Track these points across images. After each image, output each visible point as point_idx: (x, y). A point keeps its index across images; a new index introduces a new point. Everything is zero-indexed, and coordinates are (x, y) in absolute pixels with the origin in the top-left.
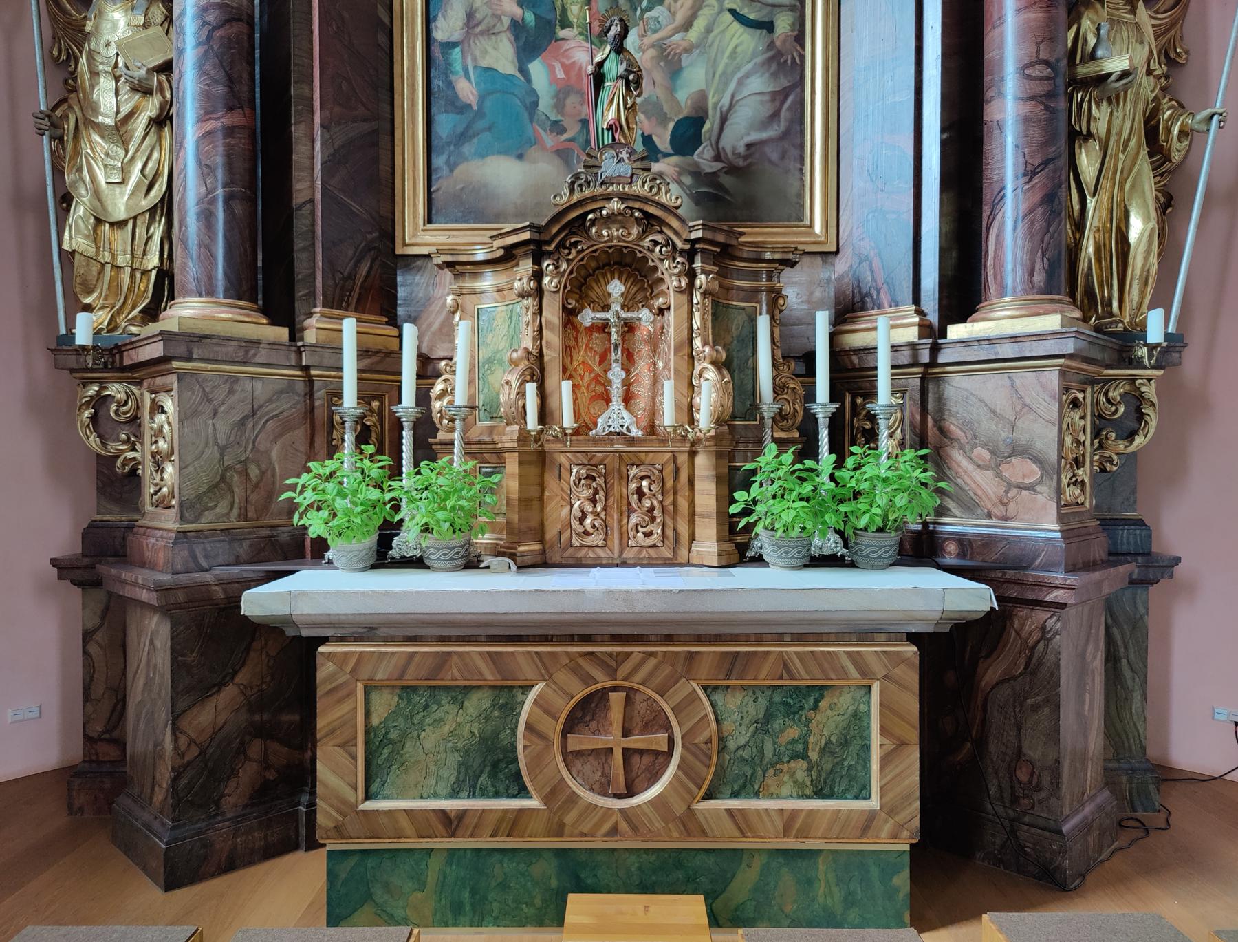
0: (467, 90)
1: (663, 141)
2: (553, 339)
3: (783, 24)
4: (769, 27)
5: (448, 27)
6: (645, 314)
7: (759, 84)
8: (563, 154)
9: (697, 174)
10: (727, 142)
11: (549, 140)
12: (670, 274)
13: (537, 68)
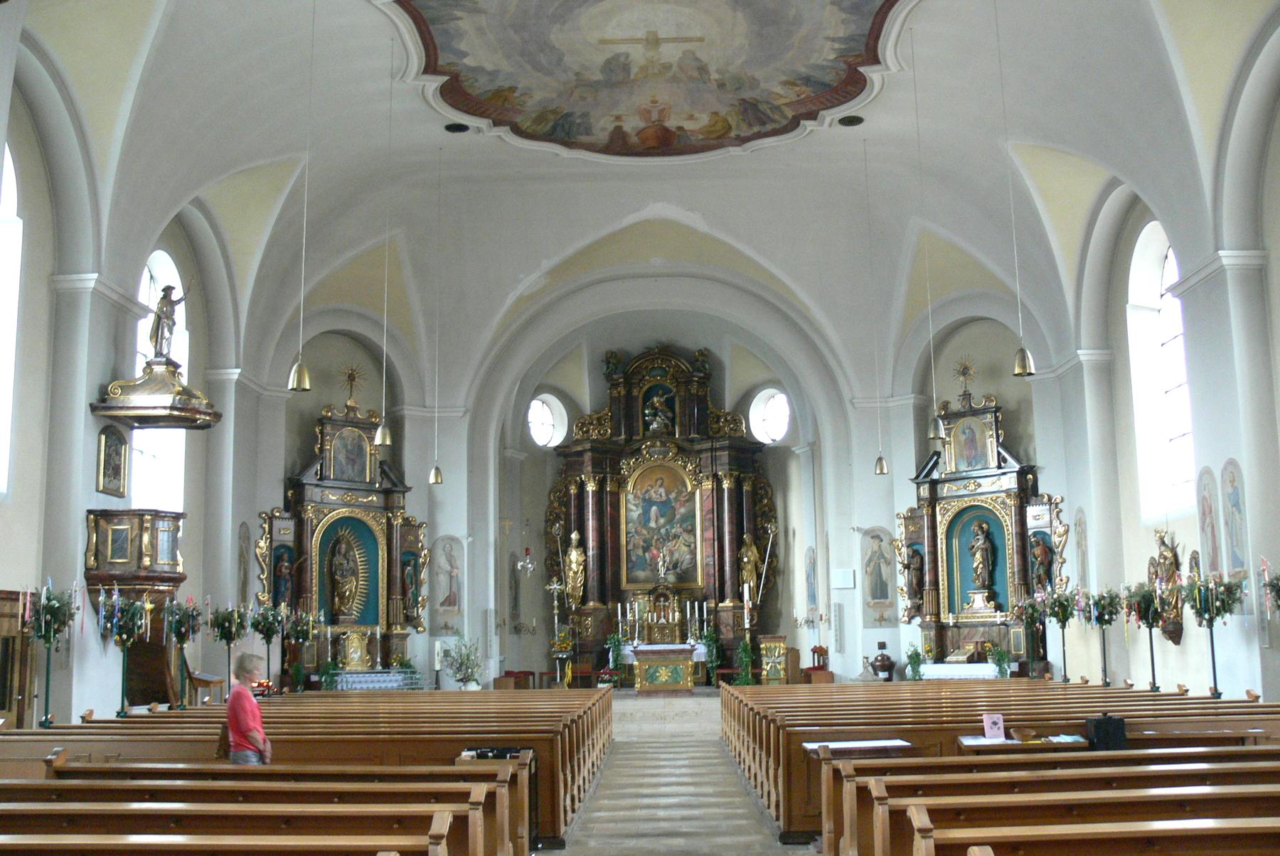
0: (634, 558)
1: (671, 567)
2: (652, 608)
3: (693, 546)
4: (689, 546)
5: (630, 547)
6: (667, 604)
7: (688, 557)
8: (652, 570)
9: (677, 573)
10: (683, 567)
11: (649, 568)
12: (671, 596)
13: (647, 555)
